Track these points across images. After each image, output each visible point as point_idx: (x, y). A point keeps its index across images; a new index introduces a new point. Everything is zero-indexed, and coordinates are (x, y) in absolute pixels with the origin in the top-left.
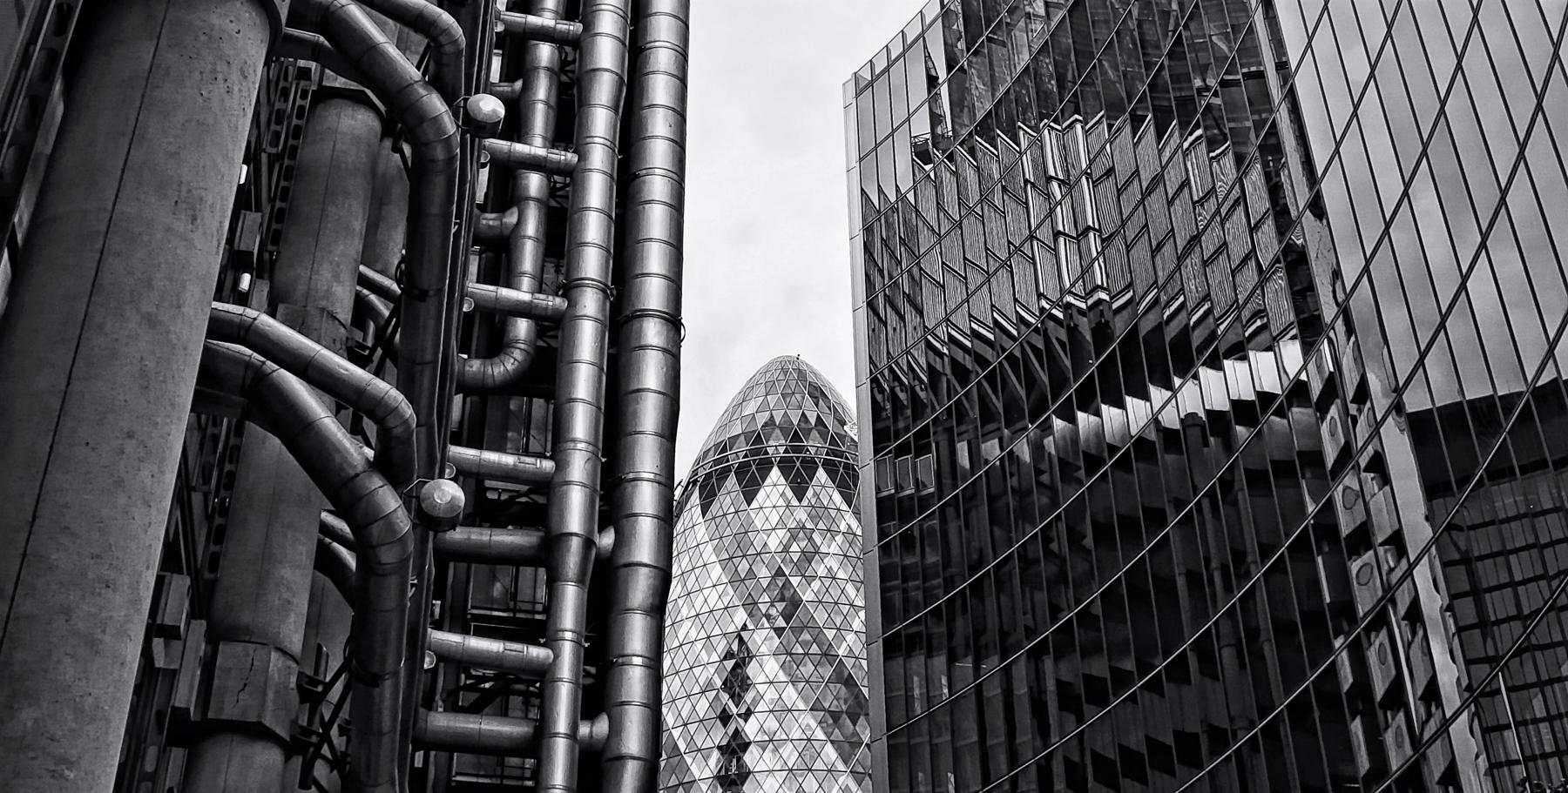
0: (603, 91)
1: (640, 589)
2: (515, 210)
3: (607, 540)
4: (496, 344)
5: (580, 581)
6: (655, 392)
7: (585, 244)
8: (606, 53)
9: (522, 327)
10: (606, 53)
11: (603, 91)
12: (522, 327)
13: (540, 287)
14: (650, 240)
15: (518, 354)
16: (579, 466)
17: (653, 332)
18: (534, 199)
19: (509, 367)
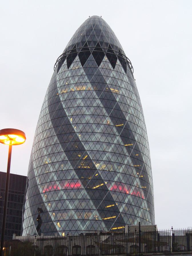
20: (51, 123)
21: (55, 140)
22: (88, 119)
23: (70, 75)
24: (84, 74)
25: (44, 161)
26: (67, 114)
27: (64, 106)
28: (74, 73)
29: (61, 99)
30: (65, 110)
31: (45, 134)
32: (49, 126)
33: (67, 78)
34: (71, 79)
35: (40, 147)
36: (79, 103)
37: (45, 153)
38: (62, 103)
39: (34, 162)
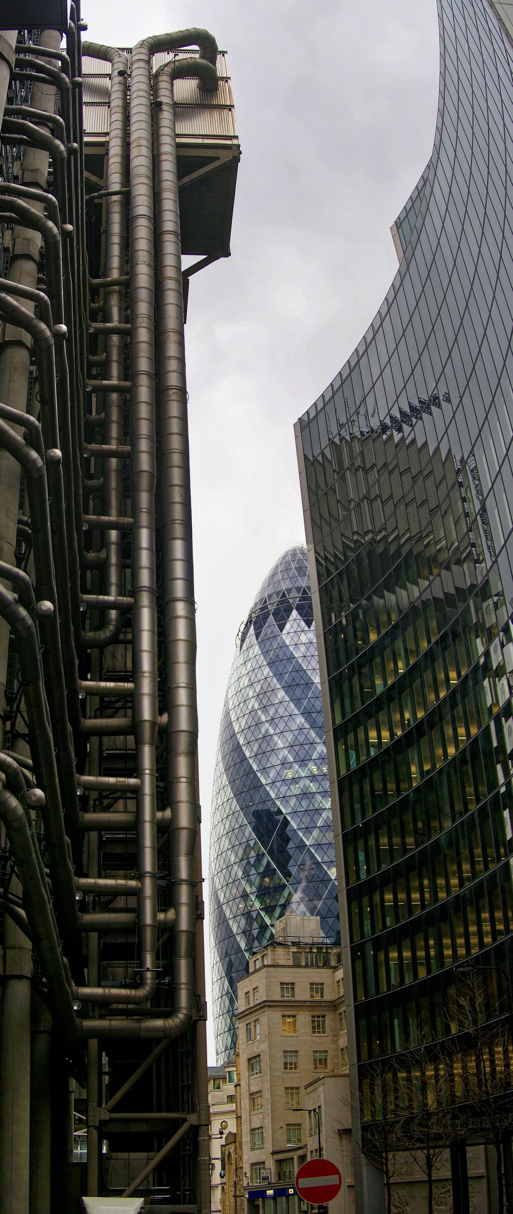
0: (144, 482)
1: (182, 743)
2: (104, 550)
3: (165, 718)
4: (102, 623)
5: (151, 744)
6: (183, 640)
7: (141, 568)
8: (145, 462)
9: (113, 614)
10: (145, 462)
11: (144, 482)
12: (113, 614)
13: (120, 593)
14: (176, 560)
15: (112, 627)
16: (146, 686)
17: (180, 608)
18: (114, 543)
19: (108, 634)
20: (235, 802)
21: (247, 834)
22: (305, 785)
23: (257, 706)
24: (287, 699)
25: (233, 875)
26: (263, 781)
27: (255, 767)
28: (264, 702)
29: (248, 754)
30: (259, 775)
31: (228, 823)
32: (233, 807)
33: (253, 714)
34: (260, 712)
35: (221, 848)
36: (284, 756)
37: (233, 859)
38: (251, 761)
39: (215, 878)
